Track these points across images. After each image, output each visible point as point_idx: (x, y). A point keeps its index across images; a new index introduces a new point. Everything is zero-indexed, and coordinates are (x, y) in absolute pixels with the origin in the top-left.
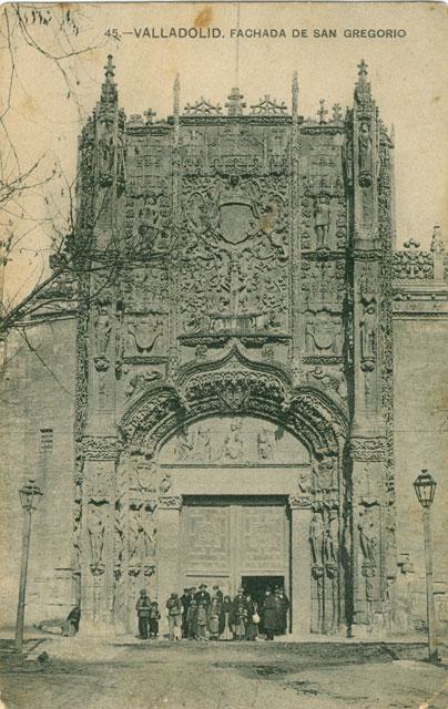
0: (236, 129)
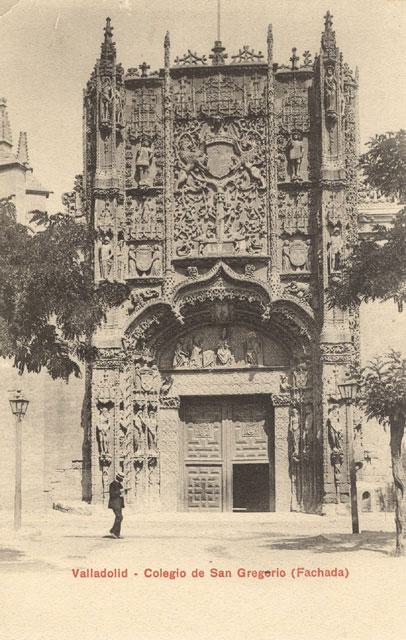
0: (220, 78)
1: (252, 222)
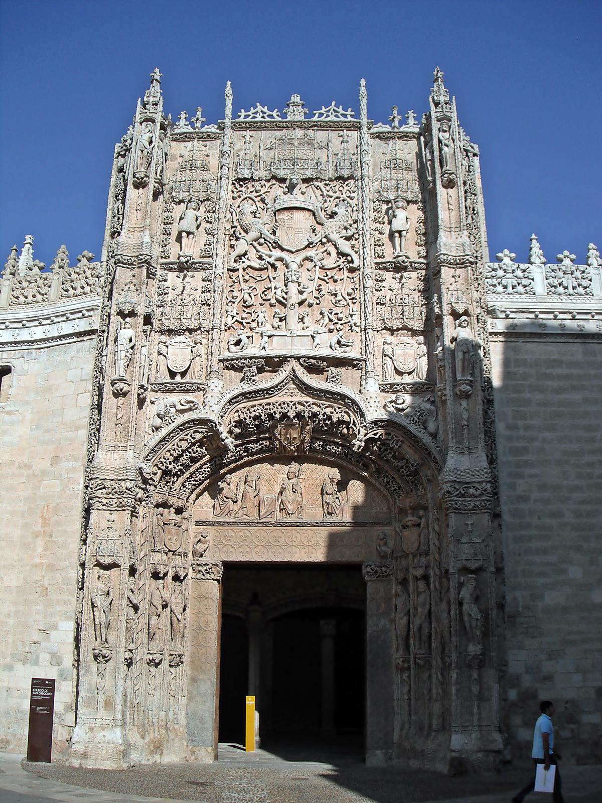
0: (299, 133)
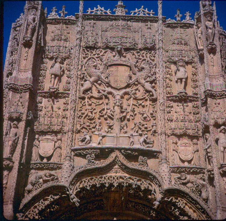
1: (145, 123)
